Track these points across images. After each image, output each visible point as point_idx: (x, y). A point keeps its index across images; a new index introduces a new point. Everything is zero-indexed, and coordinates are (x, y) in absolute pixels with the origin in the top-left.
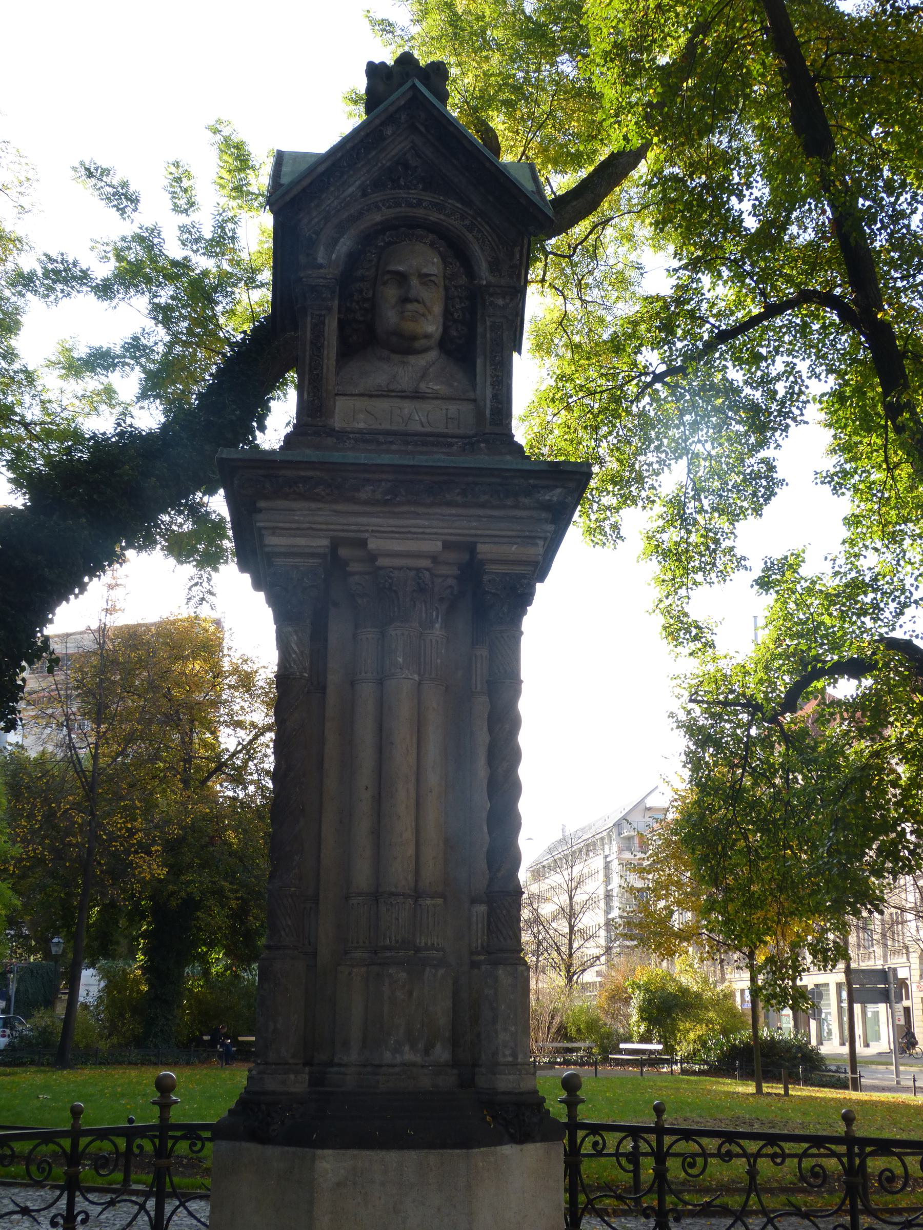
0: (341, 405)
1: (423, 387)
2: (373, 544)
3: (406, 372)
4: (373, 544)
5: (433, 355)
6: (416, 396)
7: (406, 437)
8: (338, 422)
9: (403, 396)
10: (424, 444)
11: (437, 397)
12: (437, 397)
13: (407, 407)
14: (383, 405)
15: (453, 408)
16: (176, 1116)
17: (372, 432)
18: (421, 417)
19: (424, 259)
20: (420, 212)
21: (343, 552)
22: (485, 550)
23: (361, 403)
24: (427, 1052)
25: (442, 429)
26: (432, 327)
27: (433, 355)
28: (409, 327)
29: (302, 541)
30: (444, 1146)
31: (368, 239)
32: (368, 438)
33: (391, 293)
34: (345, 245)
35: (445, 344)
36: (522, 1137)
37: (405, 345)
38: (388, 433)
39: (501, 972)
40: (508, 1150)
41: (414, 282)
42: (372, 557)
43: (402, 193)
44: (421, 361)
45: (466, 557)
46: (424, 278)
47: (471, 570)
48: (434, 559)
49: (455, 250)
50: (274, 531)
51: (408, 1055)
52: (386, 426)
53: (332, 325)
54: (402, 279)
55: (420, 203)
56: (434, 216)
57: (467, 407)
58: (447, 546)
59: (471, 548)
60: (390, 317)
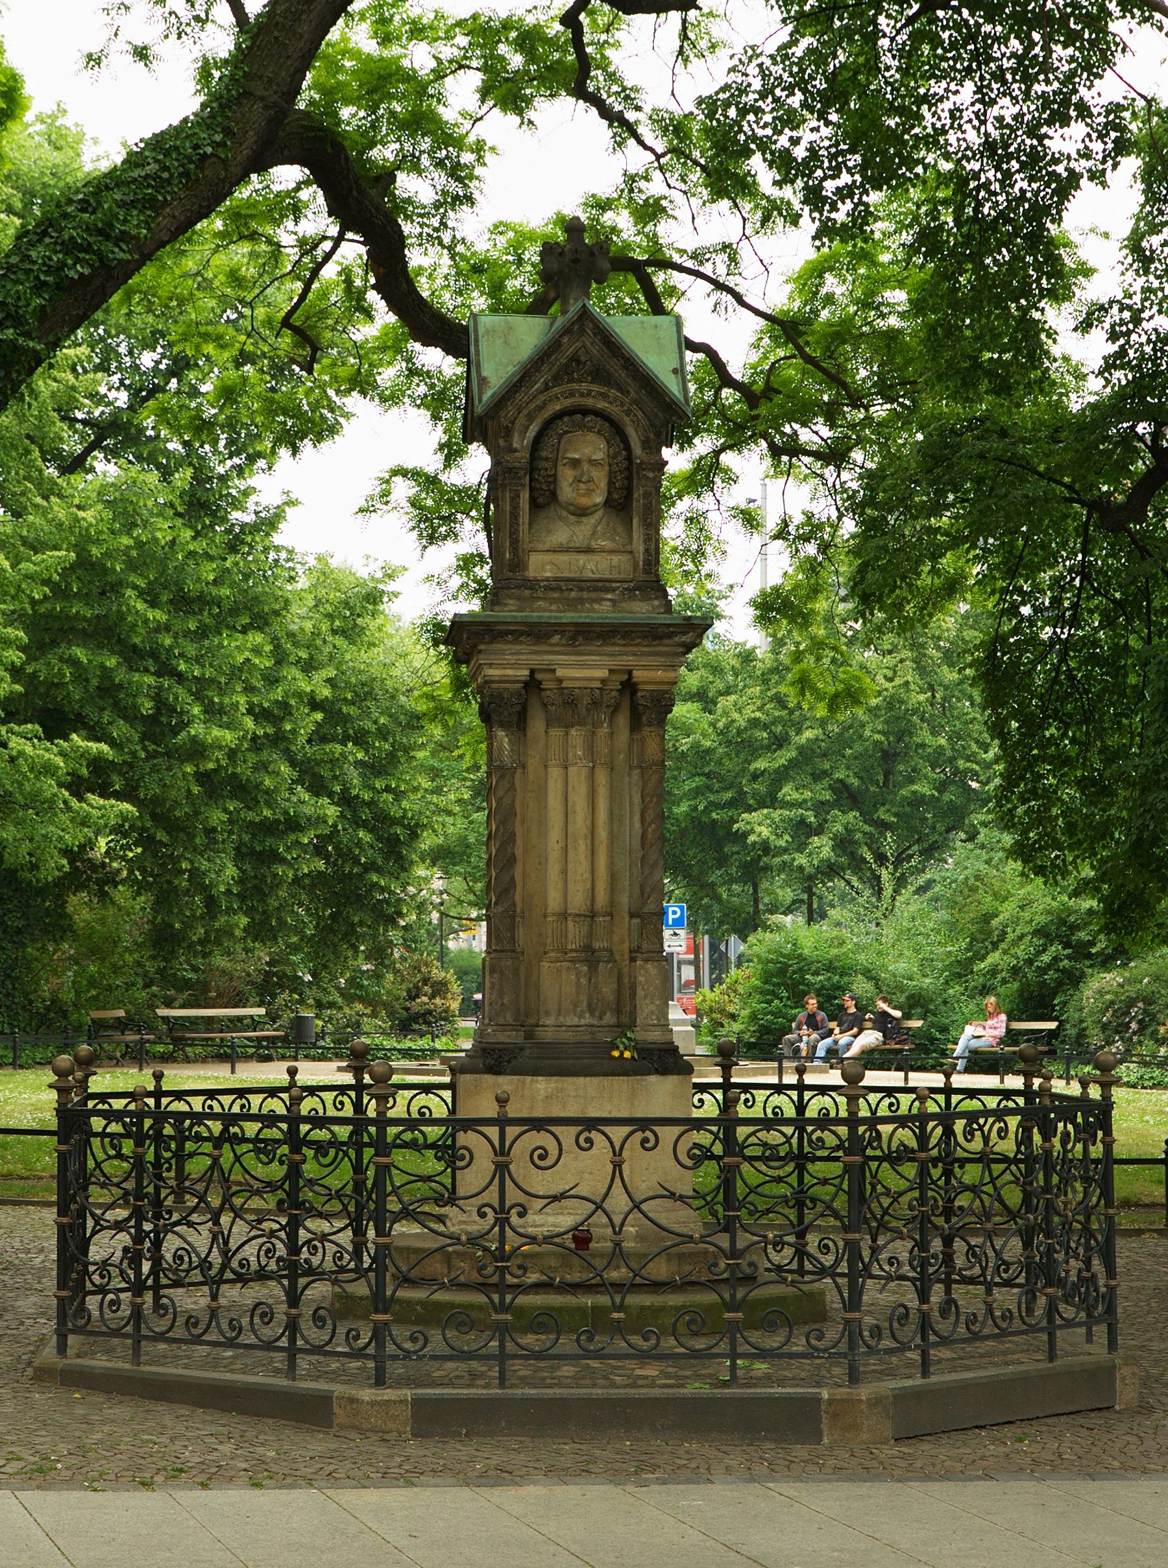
0: (534, 560)
1: (594, 544)
3: (581, 532)
4: (560, 673)
5: (599, 514)
6: (589, 550)
8: (531, 573)
9: (579, 551)
10: (596, 589)
11: (603, 551)
12: (603, 551)
13: (582, 559)
14: (563, 558)
15: (615, 559)
17: (556, 579)
18: (592, 566)
19: (591, 447)
20: (589, 402)
21: (538, 676)
23: (548, 557)
25: (607, 576)
26: (599, 499)
28: (584, 501)
29: (510, 672)
33: (566, 476)
34: (533, 430)
35: (608, 503)
36: (664, 1071)
37: (582, 512)
38: (568, 580)
39: (649, 966)
40: (653, 1079)
41: (586, 467)
42: (560, 681)
43: (575, 386)
46: (593, 463)
47: (629, 686)
48: (603, 681)
49: (616, 431)
50: (491, 665)
52: (566, 574)
53: (525, 496)
54: (575, 463)
55: (589, 394)
56: (601, 405)
57: (624, 558)
59: (630, 672)
60: (566, 491)
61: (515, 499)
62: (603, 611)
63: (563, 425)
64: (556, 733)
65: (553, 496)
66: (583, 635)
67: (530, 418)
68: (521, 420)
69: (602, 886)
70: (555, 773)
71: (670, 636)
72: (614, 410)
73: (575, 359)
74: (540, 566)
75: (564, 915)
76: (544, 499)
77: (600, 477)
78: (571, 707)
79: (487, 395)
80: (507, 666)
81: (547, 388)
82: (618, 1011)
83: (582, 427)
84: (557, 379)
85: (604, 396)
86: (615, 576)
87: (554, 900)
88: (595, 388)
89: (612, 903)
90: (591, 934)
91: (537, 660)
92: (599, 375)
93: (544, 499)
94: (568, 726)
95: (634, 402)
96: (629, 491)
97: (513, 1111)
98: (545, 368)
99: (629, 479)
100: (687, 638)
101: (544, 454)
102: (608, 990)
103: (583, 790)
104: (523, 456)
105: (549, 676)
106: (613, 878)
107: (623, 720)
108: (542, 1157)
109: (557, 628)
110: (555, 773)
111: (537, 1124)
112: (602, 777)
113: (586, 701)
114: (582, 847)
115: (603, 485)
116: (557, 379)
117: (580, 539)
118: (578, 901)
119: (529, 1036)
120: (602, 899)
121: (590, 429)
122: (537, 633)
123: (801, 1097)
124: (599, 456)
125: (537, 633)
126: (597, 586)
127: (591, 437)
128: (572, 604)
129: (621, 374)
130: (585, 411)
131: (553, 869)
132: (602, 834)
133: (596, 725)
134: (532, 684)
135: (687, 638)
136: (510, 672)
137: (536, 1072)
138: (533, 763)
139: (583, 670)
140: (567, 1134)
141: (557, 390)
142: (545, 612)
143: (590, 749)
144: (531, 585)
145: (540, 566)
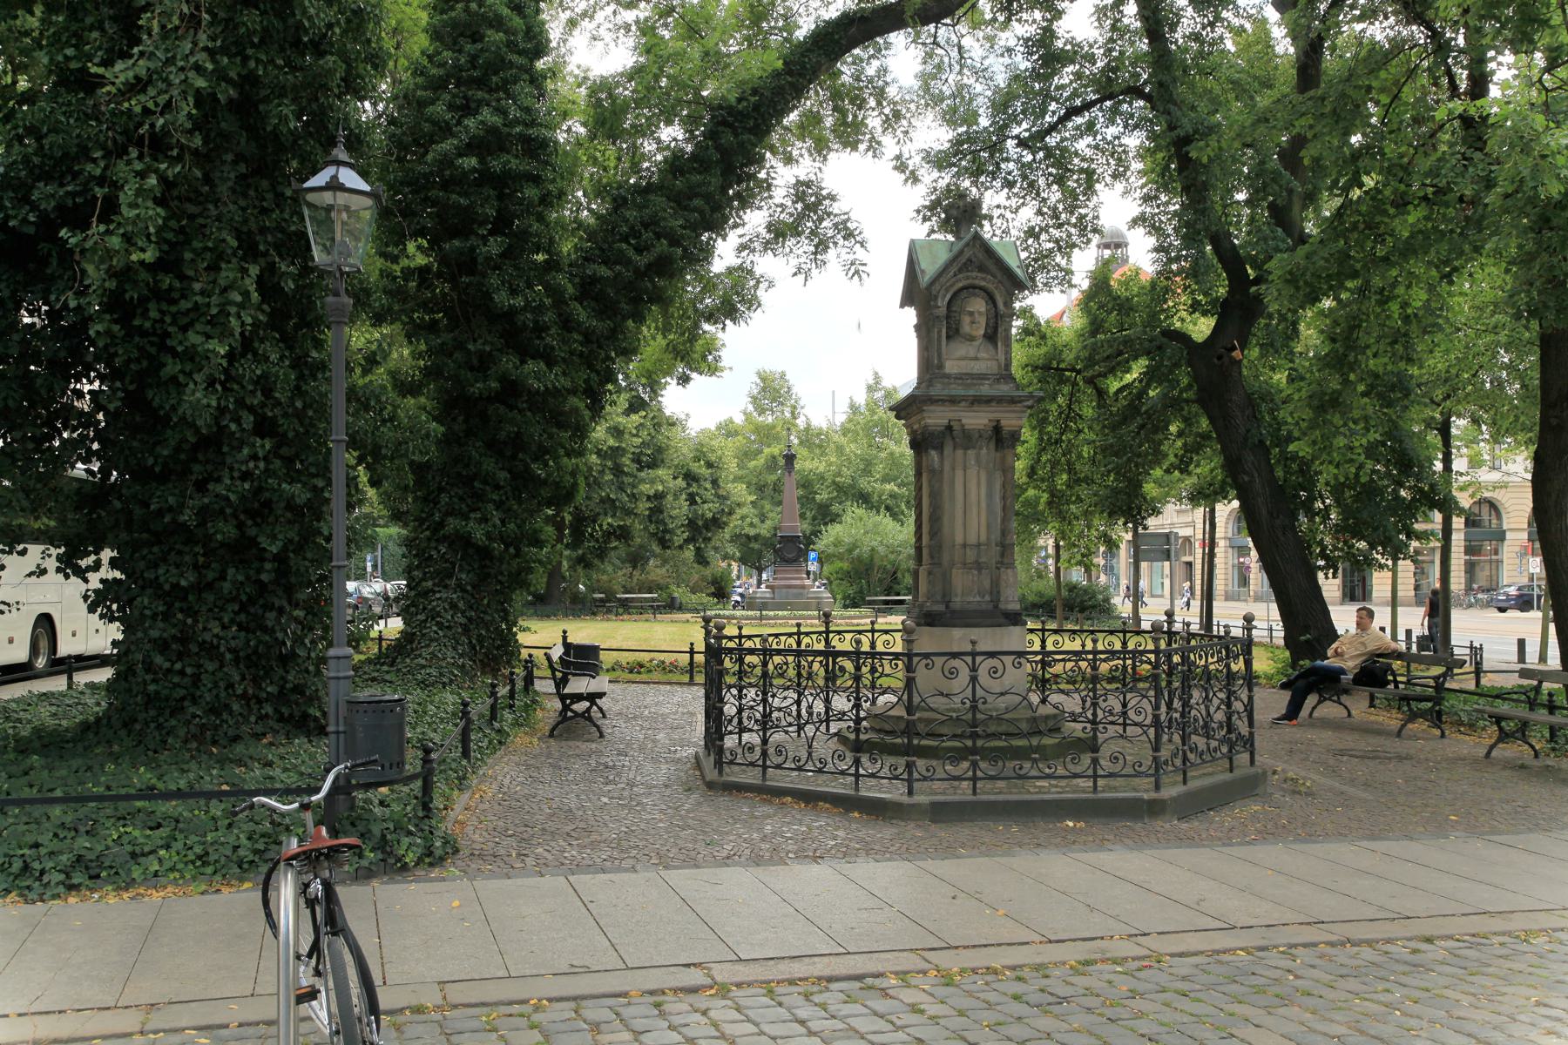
6: (976, 359)
8: (947, 370)
18: (978, 367)
19: (978, 305)
22: (1003, 423)
28: (974, 333)
32: (960, 377)
33: (966, 319)
34: (948, 297)
37: (971, 339)
44: (977, 343)
47: (997, 429)
49: (991, 299)
54: (971, 314)
56: (983, 283)
60: (966, 328)
61: (939, 332)
62: (986, 389)
63: (964, 294)
64: (960, 452)
65: (957, 331)
66: (978, 401)
67: (947, 291)
72: (990, 286)
73: (970, 260)
74: (951, 367)
75: (965, 546)
76: (954, 333)
77: (983, 321)
78: (967, 439)
79: (927, 278)
80: (936, 418)
83: (975, 295)
84: (960, 271)
87: (959, 539)
90: (979, 555)
91: (951, 415)
92: (982, 269)
93: (954, 333)
94: (966, 448)
96: (996, 328)
97: (980, 648)
102: (987, 584)
103: (974, 481)
104: (943, 311)
107: (992, 445)
109: (964, 399)
110: (959, 473)
114: (975, 510)
116: (960, 271)
117: (972, 354)
118: (972, 539)
120: (983, 538)
122: (953, 401)
124: (983, 309)
126: (982, 377)
128: (969, 386)
129: (993, 268)
130: (974, 287)
132: (983, 505)
134: (949, 428)
137: (954, 626)
138: (947, 468)
139: (977, 420)
140: (1008, 660)
142: (957, 390)
144: (948, 376)
145: (951, 367)
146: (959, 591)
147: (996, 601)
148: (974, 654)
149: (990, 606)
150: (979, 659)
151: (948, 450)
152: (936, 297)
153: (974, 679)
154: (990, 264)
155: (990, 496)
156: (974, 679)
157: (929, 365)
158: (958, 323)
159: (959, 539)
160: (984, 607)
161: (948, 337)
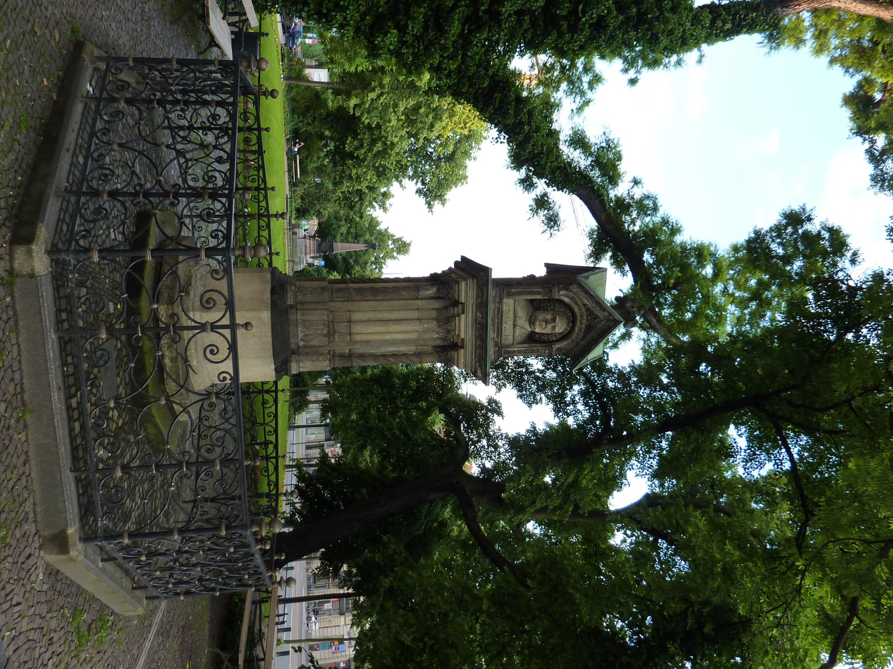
2: (463, 316)
4: (463, 316)
6: (515, 326)
7: (500, 323)
8: (505, 300)
13: (511, 323)
14: (511, 315)
15: (511, 337)
16: (273, 221)
18: (507, 327)
19: (560, 327)
20: (578, 324)
21: (460, 306)
22: (462, 351)
23: (512, 309)
24: (302, 340)
26: (537, 330)
27: (530, 329)
28: (537, 323)
29: (463, 293)
30: (274, 349)
31: (568, 306)
32: (500, 312)
34: (567, 300)
36: (276, 370)
37: (532, 322)
39: (327, 362)
40: (273, 367)
42: (459, 316)
45: (460, 344)
46: (554, 327)
48: (459, 335)
49: (564, 337)
50: (466, 285)
51: (300, 335)
52: (504, 316)
53: (539, 297)
54: (554, 320)
56: (577, 329)
57: (511, 342)
58: (463, 339)
59: (462, 347)
60: (541, 316)
62: (491, 335)
64: (434, 314)
66: (481, 328)
67: (572, 299)
68: (571, 294)
69: (364, 337)
70: (416, 314)
71: (480, 366)
72: (574, 335)
73: (596, 317)
74: (508, 304)
75: (350, 321)
76: (535, 306)
77: (548, 330)
79: (583, 279)
80: (466, 292)
81: (584, 305)
82: (305, 347)
83: (568, 323)
84: (588, 310)
85: (580, 330)
86: (503, 338)
87: (356, 316)
88: (584, 326)
89: (356, 342)
92: (589, 328)
94: (438, 320)
95: (578, 344)
97: (240, 332)
98: (594, 305)
99: (544, 342)
100: (479, 374)
101: (557, 305)
103: (409, 328)
105: (460, 311)
106: (367, 342)
107: (439, 342)
108: (212, 352)
110: (416, 314)
111: (233, 348)
112: (413, 336)
113: (450, 328)
115: (544, 332)
119: (291, 307)
120: (357, 338)
121: (568, 325)
122: (482, 306)
123: (272, 391)
125: (482, 306)
126: (499, 330)
127: (565, 326)
129: (589, 337)
131: (371, 315)
132: (387, 337)
133: (438, 333)
134: (456, 303)
135: (479, 374)
136: (463, 293)
138: (419, 303)
139: (464, 327)
141: (583, 310)
143: (427, 330)
146: (307, 317)
147: (296, 352)
148: (233, 326)
149: (293, 346)
150: (227, 332)
151: (437, 304)
152: (567, 289)
153: (202, 327)
154: (592, 334)
155: (394, 343)
156: (202, 327)
157: (508, 286)
158: (545, 310)
159: (356, 316)
160: (292, 340)
161: (532, 301)
